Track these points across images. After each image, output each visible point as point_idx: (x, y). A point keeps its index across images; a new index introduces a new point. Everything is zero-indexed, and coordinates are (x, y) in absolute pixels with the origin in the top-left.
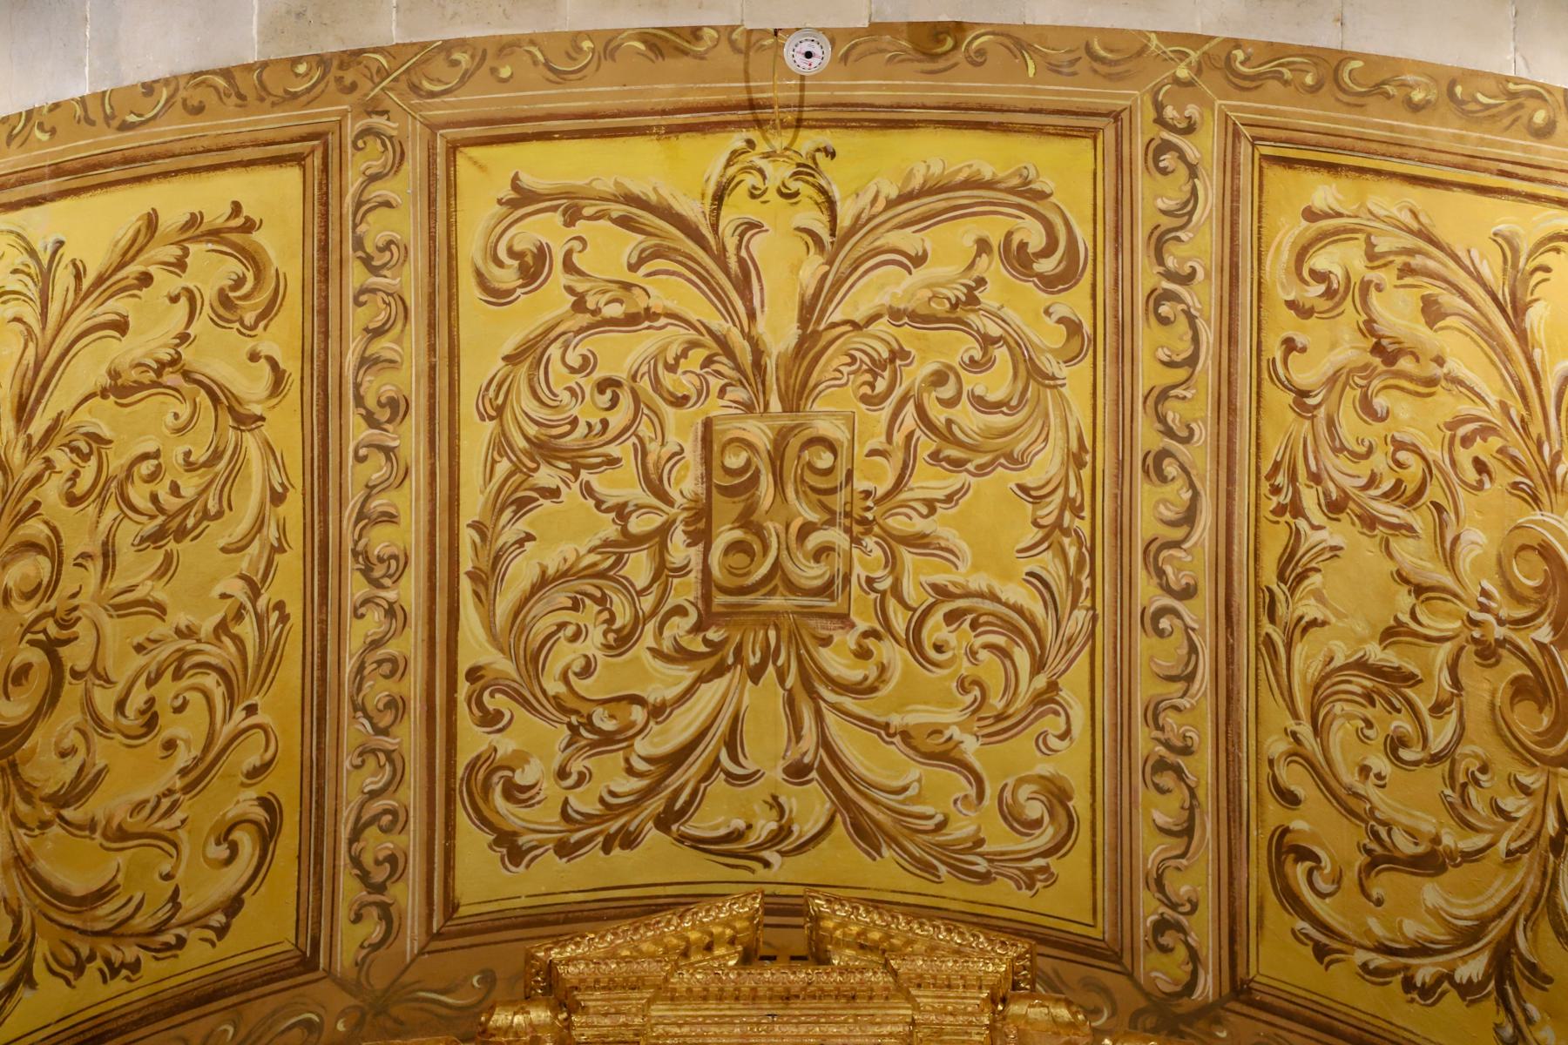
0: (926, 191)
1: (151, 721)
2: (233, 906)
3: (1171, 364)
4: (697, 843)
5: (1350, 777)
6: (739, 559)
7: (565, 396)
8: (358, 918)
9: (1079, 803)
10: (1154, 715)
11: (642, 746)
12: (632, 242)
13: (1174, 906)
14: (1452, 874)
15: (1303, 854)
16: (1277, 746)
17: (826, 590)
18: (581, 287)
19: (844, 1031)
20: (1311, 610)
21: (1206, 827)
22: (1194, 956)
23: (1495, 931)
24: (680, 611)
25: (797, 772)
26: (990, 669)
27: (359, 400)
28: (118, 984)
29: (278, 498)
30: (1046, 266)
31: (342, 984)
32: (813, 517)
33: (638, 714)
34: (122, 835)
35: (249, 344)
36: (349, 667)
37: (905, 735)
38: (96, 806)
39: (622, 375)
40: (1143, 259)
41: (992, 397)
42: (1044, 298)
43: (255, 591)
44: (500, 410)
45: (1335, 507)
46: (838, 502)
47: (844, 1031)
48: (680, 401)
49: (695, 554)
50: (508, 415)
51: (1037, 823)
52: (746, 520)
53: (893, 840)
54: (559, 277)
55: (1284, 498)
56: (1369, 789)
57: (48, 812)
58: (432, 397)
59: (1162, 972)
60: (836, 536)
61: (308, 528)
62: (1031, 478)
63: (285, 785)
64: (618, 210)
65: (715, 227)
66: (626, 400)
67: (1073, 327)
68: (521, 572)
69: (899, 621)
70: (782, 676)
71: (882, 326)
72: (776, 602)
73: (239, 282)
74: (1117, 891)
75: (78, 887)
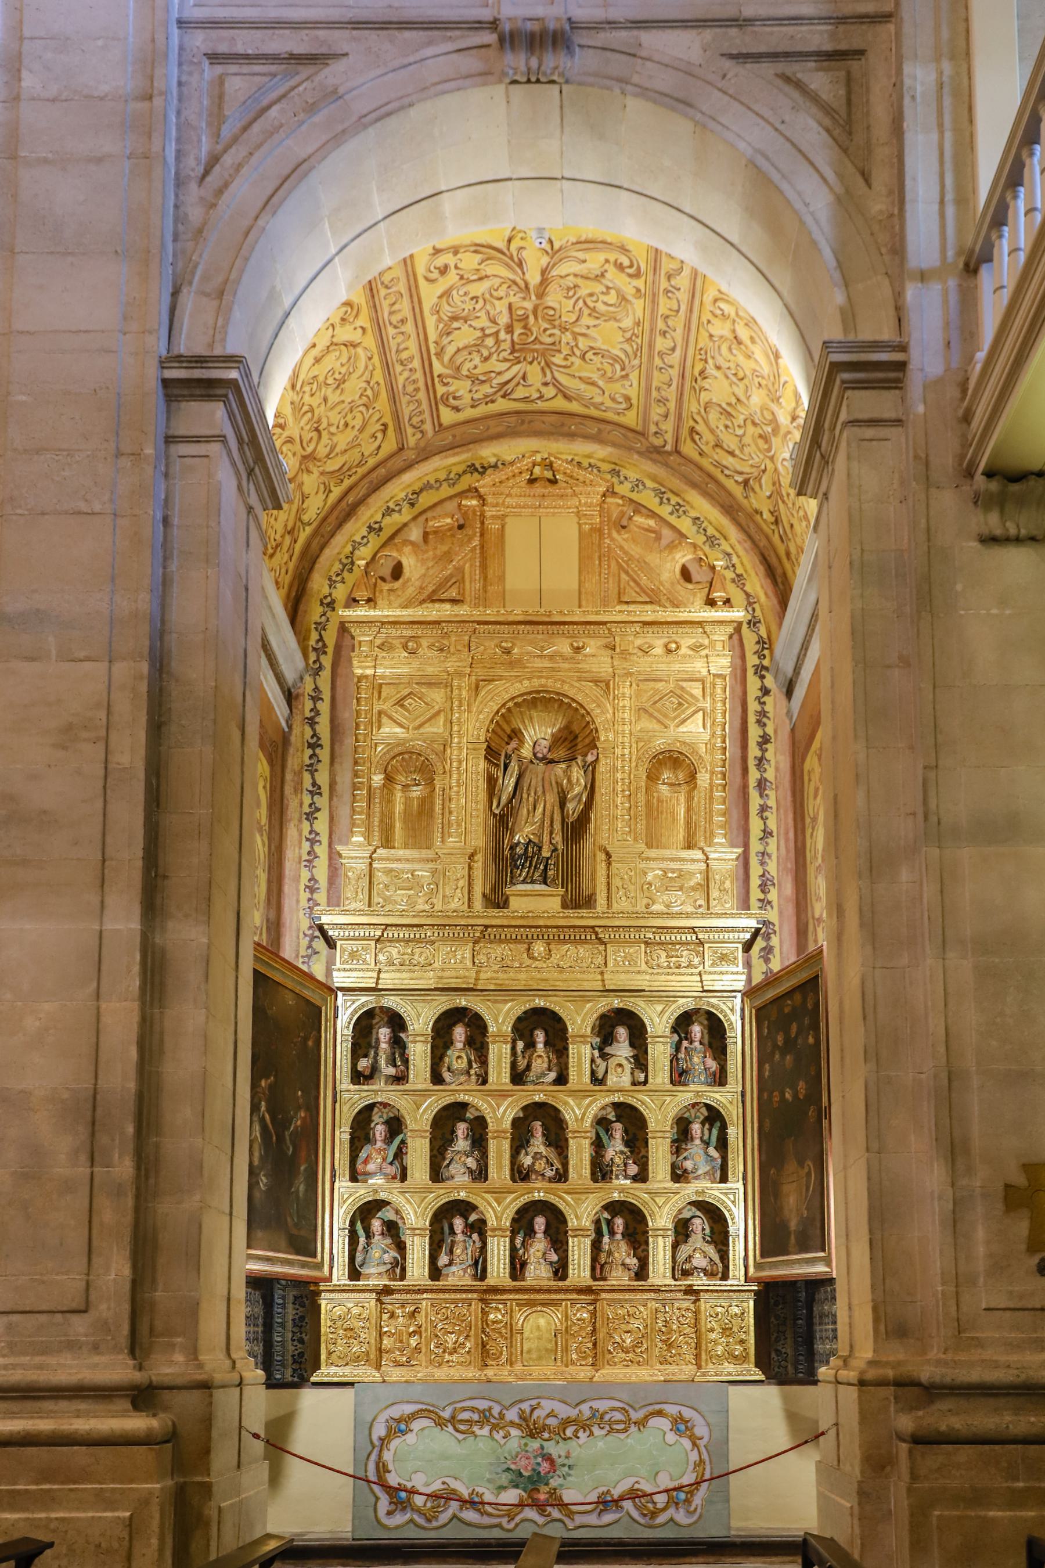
0: (586, 242)
3: (671, 310)
4: (515, 400)
6: (524, 337)
7: (460, 304)
11: (495, 382)
12: (478, 257)
17: (554, 344)
18: (461, 273)
20: (707, 386)
23: (746, 476)
24: (504, 350)
25: (546, 384)
26: (609, 369)
27: (391, 324)
29: (370, 359)
30: (630, 271)
32: (548, 326)
33: (493, 375)
35: (353, 327)
36: (400, 387)
37: (580, 378)
38: (338, 450)
39: (479, 294)
40: (663, 279)
41: (610, 302)
42: (628, 280)
43: (368, 382)
44: (438, 312)
45: (718, 368)
46: (557, 323)
48: (500, 299)
49: (508, 337)
50: (441, 313)
52: (525, 327)
53: (576, 400)
54: (453, 271)
55: (703, 357)
58: (414, 315)
60: (556, 331)
61: (381, 361)
62: (623, 325)
63: (388, 419)
64: (473, 248)
65: (508, 249)
66: (481, 301)
67: (638, 290)
68: (450, 350)
69: (578, 353)
70: (539, 363)
71: (571, 278)
72: (537, 347)
73: (346, 312)
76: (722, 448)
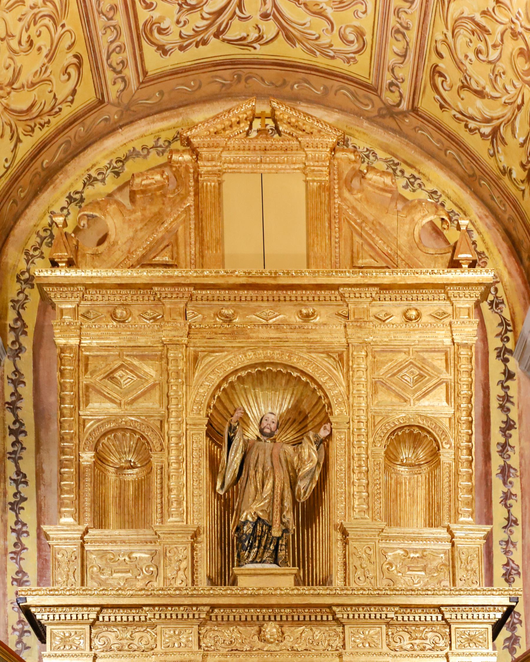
1: (31, 43)
2: (74, 92)
5: (462, 57)
8: (115, 83)
9: (368, 38)
10: (397, 12)
13: (396, 79)
14: (486, 100)
15: (441, 75)
16: (439, 37)
19: (283, 167)
21: (411, 55)
22: (401, 96)
23: (495, 123)
25: (265, 16)
28: (46, 129)
31: (113, 105)
34: (33, 84)
47: (283, 167)
51: (352, 42)
56: (466, 62)
57: (8, 89)
59: (390, 98)
74: (378, 70)
75: (25, 107)
76: (469, 88)
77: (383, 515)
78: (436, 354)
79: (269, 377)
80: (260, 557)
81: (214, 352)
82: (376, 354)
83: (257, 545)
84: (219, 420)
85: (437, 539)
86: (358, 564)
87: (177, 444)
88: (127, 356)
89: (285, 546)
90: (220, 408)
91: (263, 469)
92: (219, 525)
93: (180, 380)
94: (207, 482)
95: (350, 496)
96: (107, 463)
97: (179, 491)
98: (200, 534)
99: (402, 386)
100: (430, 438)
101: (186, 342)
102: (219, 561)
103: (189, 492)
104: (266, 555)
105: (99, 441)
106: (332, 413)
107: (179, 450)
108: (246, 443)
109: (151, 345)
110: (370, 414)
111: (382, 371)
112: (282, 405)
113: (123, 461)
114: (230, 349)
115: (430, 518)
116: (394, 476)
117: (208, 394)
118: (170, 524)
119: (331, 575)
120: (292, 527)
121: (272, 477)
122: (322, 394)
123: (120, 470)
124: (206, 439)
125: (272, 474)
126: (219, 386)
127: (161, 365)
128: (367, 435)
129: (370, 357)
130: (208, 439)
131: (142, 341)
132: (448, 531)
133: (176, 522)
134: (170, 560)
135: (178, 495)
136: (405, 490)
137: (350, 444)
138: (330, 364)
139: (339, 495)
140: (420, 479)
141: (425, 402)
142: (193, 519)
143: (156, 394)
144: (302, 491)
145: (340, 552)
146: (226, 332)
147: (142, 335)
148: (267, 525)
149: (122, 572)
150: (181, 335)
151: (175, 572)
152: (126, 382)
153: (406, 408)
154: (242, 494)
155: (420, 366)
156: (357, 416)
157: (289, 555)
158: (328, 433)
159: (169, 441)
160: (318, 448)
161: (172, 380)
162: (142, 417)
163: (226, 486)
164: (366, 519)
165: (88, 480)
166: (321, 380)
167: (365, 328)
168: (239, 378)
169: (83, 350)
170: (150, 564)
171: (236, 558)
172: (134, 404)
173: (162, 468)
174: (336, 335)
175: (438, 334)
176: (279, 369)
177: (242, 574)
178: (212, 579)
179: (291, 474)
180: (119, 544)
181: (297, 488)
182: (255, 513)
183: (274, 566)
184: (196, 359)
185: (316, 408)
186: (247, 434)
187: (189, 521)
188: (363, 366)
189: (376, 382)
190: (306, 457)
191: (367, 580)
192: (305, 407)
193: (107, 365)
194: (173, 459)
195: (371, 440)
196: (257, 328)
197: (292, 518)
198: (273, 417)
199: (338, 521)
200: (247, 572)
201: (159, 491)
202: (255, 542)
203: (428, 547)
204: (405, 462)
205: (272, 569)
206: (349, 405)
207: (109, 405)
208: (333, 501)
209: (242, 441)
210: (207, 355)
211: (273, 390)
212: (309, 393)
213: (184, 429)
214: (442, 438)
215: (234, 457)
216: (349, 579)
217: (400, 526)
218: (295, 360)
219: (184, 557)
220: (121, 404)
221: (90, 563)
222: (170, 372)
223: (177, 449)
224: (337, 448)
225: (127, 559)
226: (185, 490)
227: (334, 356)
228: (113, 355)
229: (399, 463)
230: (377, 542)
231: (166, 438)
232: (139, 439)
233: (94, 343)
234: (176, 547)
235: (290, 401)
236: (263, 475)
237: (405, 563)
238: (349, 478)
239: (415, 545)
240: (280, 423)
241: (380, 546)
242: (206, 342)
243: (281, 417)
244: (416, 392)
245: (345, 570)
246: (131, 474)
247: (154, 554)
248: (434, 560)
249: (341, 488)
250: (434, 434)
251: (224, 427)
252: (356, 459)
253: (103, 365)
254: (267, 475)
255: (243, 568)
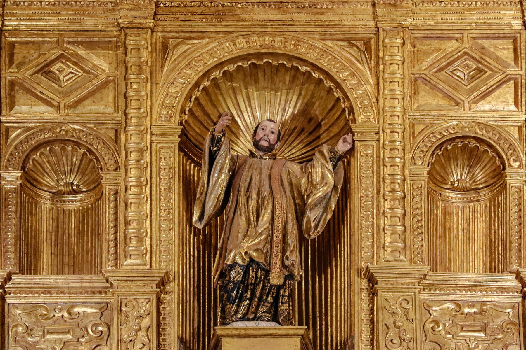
77: (425, 256)
78: (500, 41)
79: (268, 71)
80: (252, 313)
81: (190, 38)
82: (416, 42)
83: (249, 296)
84: (197, 130)
85: (502, 289)
86: (390, 321)
87: (138, 161)
88: (69, 43)
89: (289, 297)
90: (199, 113)
91: (258, 195)
92: (196, 270)
93: (143, 76)
94: (179, 212)
95: (380, 230)
96: (39, 186)
97: (141, 224)
98: (169, 282)
99: (453, 85)
100: (491, 154)
101: (151, 25)
102: (196, 318)
103: (154, 225)
104: (261, 309)
105: (28, 157)
106: (354, 121)
107: (141, 169)
108: (234, 160)
109: (103, 29)
110: (407, 122)
111: (425, 65)
112: (284, 109)
113: (63, 184)
114: (213, 34)
115: (492, 260)
116: (441, 204)
117: (182, 94)
118: (128, 268)
119: (352, 337)
120: (298, 272)
121: (270, 205)
122: (341, 95)
123: (57, 195)
124: (179, 155)
125: (270, 201)
126: (197, 85)
127: (117, 55)
128: (403, 150)
129: (408, 46)
130: (182, 154)
131: (89, 23)
132: (517, 278)
133: (136, 265)
134: (127, 316)
135: (139, 230)
136: (457, 223)
137: (379, 162)
138: (352, 55)
139: (364, 230)
140: (478, 208)
141: (485, 106)
142: (160, 262)
143: (109, 94)
144: (313, 225)
145: (365, 306)
146: (207, 11)
147: (90, 15)
148: (263, 269)
149: (58, 333)
150: (145, 15)
151: (134, 333)
152: (67, 78)
153: (458, 114)
154: (228, 228)
155: (478, 57)
156: (390, 124)
157: (293, 310)
158: (349, 147)
159: (126, 157)
160: (334, 167)
161: (132, 76)
162: (89, 125)
163: (206, 217)
164: (401, 261)
165: (12, 208)
166: (340, 76)
167: (402, 7)
168: (225, 73)
169: (7, 34)
170: (99, 321)
171: (219, 314)
172: (79, 107)
173: (116, 193)
174: (361, 17)
175: (504, 15)
176: (280, 62)
177: (228, 336)
178: (186, 342)
179: (297, 201)
180: (55, 295)
181: (305, 221)
182: (246, 253)
183: (273, 324)
184: (165, 48)
185: (332, 113)
186: (236, 148)
187: (154, 264)
188: (398, 58)
189: (416, 80)
190: (318, 179)
191: (403, 343)
192: (317, 113)
193: (40, 55)
194: (132, 180)
195: (408, 156)
196: (250, 7)
197: (298, 260)
198: (272, 125)
199: (363, 265)
200: (234, 332)
201: (112, 224)
202: (247, 292)
203: (489, 299)
204: (456, 185)
205: (270, 329)
206: (379, 110)
207: (42, 108)
208: (355, 237)
209: (228, 157)
210: (181, 43)
211: (272, 90)
212: (323, 94)
213: (149, 141)
214: (509, 154)
215: (218, 179)
216: (378, 342)
217: (450, 271)
218: (304, 50)
219: (146, 312)
220: (59, 107)
221: (13, 321)
222: (129, 65)
223: (139, 168)
224: (361, 166)
225: (66, 315)
226: (148, 222)
227: (358, 44)
228: (49, 42)
229: (448, 187)
230: (417, 292)
231: (123, 152)
232: (84, 154)
233: (23, 25)
234: (135, 299)
235: (296, 104)
236: (258, 202)
237: (457, 320)
238: (378, 206)
239: (470, 297)
240: (282, 133)
241: (422, 297)
242: (180, 26)
243: (283, 125)
244: (473, 92)
245: (373, 330)
246: (72, 201)
247: (103, 309)
248: (498, 317)
249: (367, 221)
250: (498, 148)
251: (204, 139)
252: (388, 181)
253: (35, 56)
254: (263, 202)
255: (228, 327)
